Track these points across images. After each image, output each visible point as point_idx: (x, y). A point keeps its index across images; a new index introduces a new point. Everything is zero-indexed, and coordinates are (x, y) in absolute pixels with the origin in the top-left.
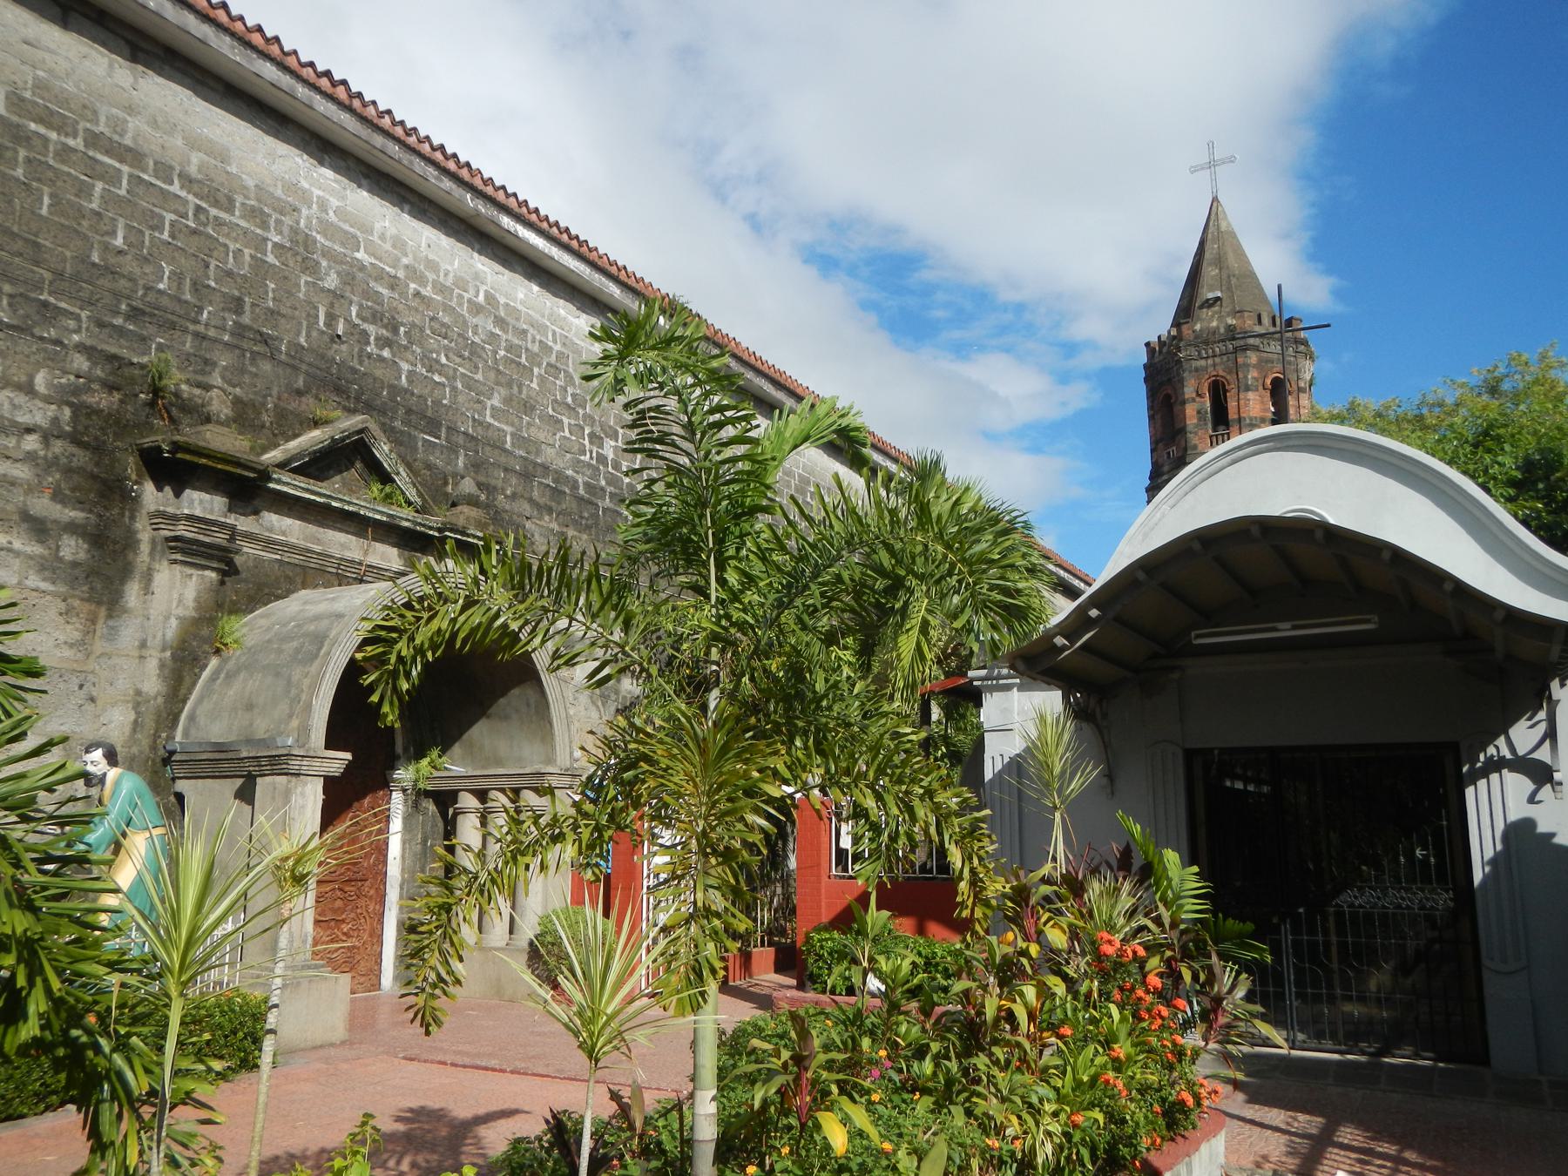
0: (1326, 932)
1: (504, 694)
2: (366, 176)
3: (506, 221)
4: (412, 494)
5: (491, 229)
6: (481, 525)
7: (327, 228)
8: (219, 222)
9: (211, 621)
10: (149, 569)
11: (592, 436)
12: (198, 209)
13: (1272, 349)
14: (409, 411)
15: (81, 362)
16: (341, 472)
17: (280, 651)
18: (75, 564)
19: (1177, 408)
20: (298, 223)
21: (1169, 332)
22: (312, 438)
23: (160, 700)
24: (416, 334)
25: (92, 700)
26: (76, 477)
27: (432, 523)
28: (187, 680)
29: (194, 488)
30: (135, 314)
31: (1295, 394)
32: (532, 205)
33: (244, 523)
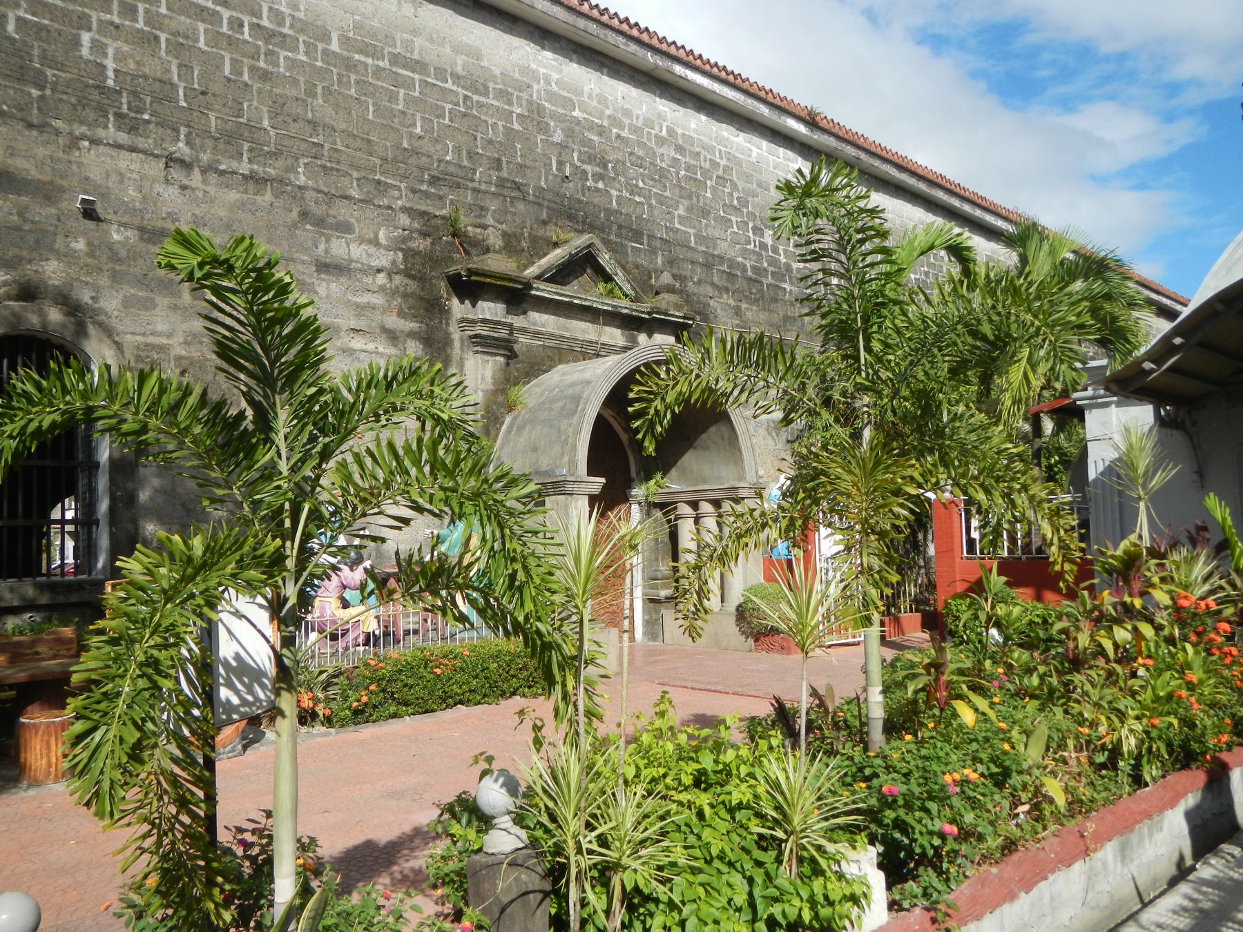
1: (705, 430)
2: (575, 52)
3: (678, 69)
4: (627, 288)
5: (667, 77)
6: (678, 308)
7: (551, 97)
8: (480, 105)
9: (504, 391)
11: (755, 229)
12: (466, 97)
14: (620, 227)
15: (404, 220)
20: (531, 96)
22: (555, 256)
24: (620, 166)
26: (410, 300)
27: (643, 308)
30: (434, 181)
32: (696, 53)
33: (518, 321)
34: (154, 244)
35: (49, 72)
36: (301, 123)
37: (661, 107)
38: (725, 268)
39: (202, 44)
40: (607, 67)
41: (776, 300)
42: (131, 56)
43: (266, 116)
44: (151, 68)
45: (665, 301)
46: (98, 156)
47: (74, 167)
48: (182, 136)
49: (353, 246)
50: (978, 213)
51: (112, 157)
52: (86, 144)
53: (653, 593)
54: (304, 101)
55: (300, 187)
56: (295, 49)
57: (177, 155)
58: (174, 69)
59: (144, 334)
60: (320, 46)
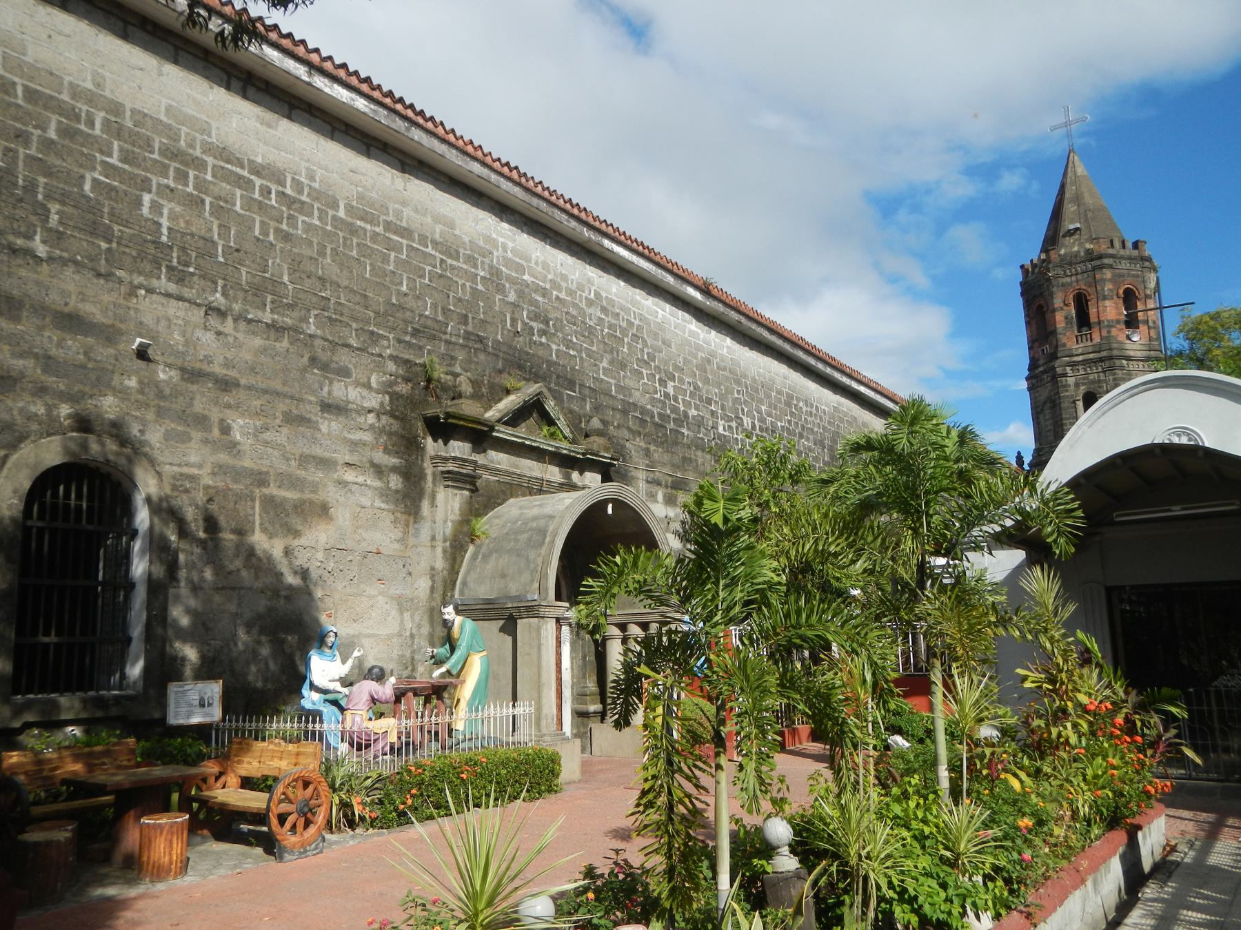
0: (1209, 704)
2: (525, 224)
3: (607, 243)
4: (567, 432)
5: (597, 249)
6: (607, 450)
7: (508, 262)
8: (453, 268)
9: (468, 522)
11: (661, 380)
12: (442, 261)
14: (558, 377)
15: (391, 367)
16: (525, 420)
17: (517, 540)
18: (397, 491)
19: (1048, 316)
20: (492, 261)
21: (1039, 257)
22: (509, 403)
23: (445, 573)
24: (558, 324)
25: (410, 574)
26: (394, 438)
27: (578, 450)
28: (459, 559)
30: (416, 333)
31: (1143, 300)
32: (621, 230)
33: (480, 459)
34: (192, 383)
35: (116, 228)
36: (314, 280)
37: (590, 274)
38: (638, 414)
39: (238, 208)
40: (550, 238)
41: (676, 443)
42: (182, 216)
43: (286, 272)
44: (197, 227)
45: (597, 442)
46: (151, 303)
47: (132, 312)
48: (219, 288)
49: (350, 389)
50: (829, 370)
51: (163, 305)
52: (143, 292)
53: (581, 708)
54: (316, 260)
55: (311, 336)
56: (310, 215)
57: (215, 304)
58: (215, 229)
59: (179, 465)
60: (331, 213)
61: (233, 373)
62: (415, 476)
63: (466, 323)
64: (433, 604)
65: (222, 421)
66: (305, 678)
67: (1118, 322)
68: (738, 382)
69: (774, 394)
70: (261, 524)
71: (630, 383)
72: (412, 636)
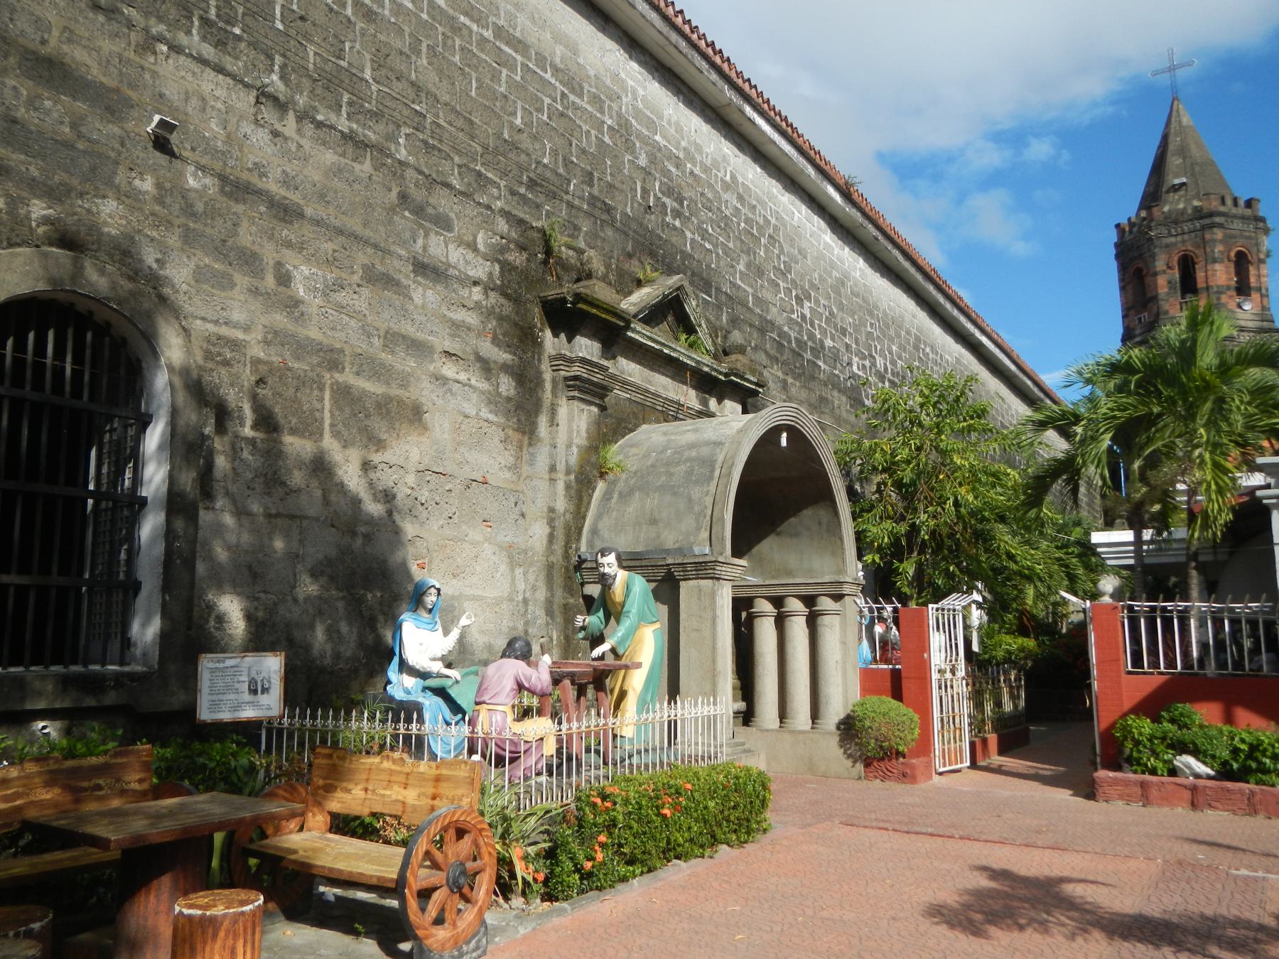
1: (795, 509)
3: (748, 110)
5: (734, 117)
6: (753, 372)
7: (638, 114)
10: (553, 404)
11: (797, 297)
12: (563, 94)
13: (1235, 226)
15: (502, 225)
17: (672, 474)
18: (509, 399)
19: (1148, 280)
23: (568, 516)
25: (523, 515)
29: (582, 336)
31: (1255, 265)
32: (765, 97)
34: (237, 201)
41: (813, 378)
43: (368, 65)
51: (194, 74)
52: (165, 48)
55: (400, 162)
59: (216, 322)
61: (295, 197)
62: (531, 381)
63: (591, 186)
64: (552, 558)
65: (279, 265)
66: (391, 654)
67: (1229, 288)
68: (871, 314)
69: (903, 333)
70: (332, 425)
71: (767, 295)
72: (525, 601)
